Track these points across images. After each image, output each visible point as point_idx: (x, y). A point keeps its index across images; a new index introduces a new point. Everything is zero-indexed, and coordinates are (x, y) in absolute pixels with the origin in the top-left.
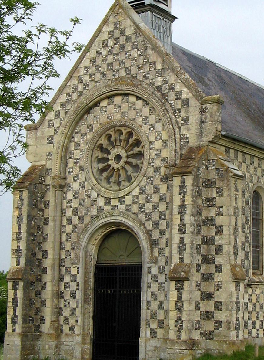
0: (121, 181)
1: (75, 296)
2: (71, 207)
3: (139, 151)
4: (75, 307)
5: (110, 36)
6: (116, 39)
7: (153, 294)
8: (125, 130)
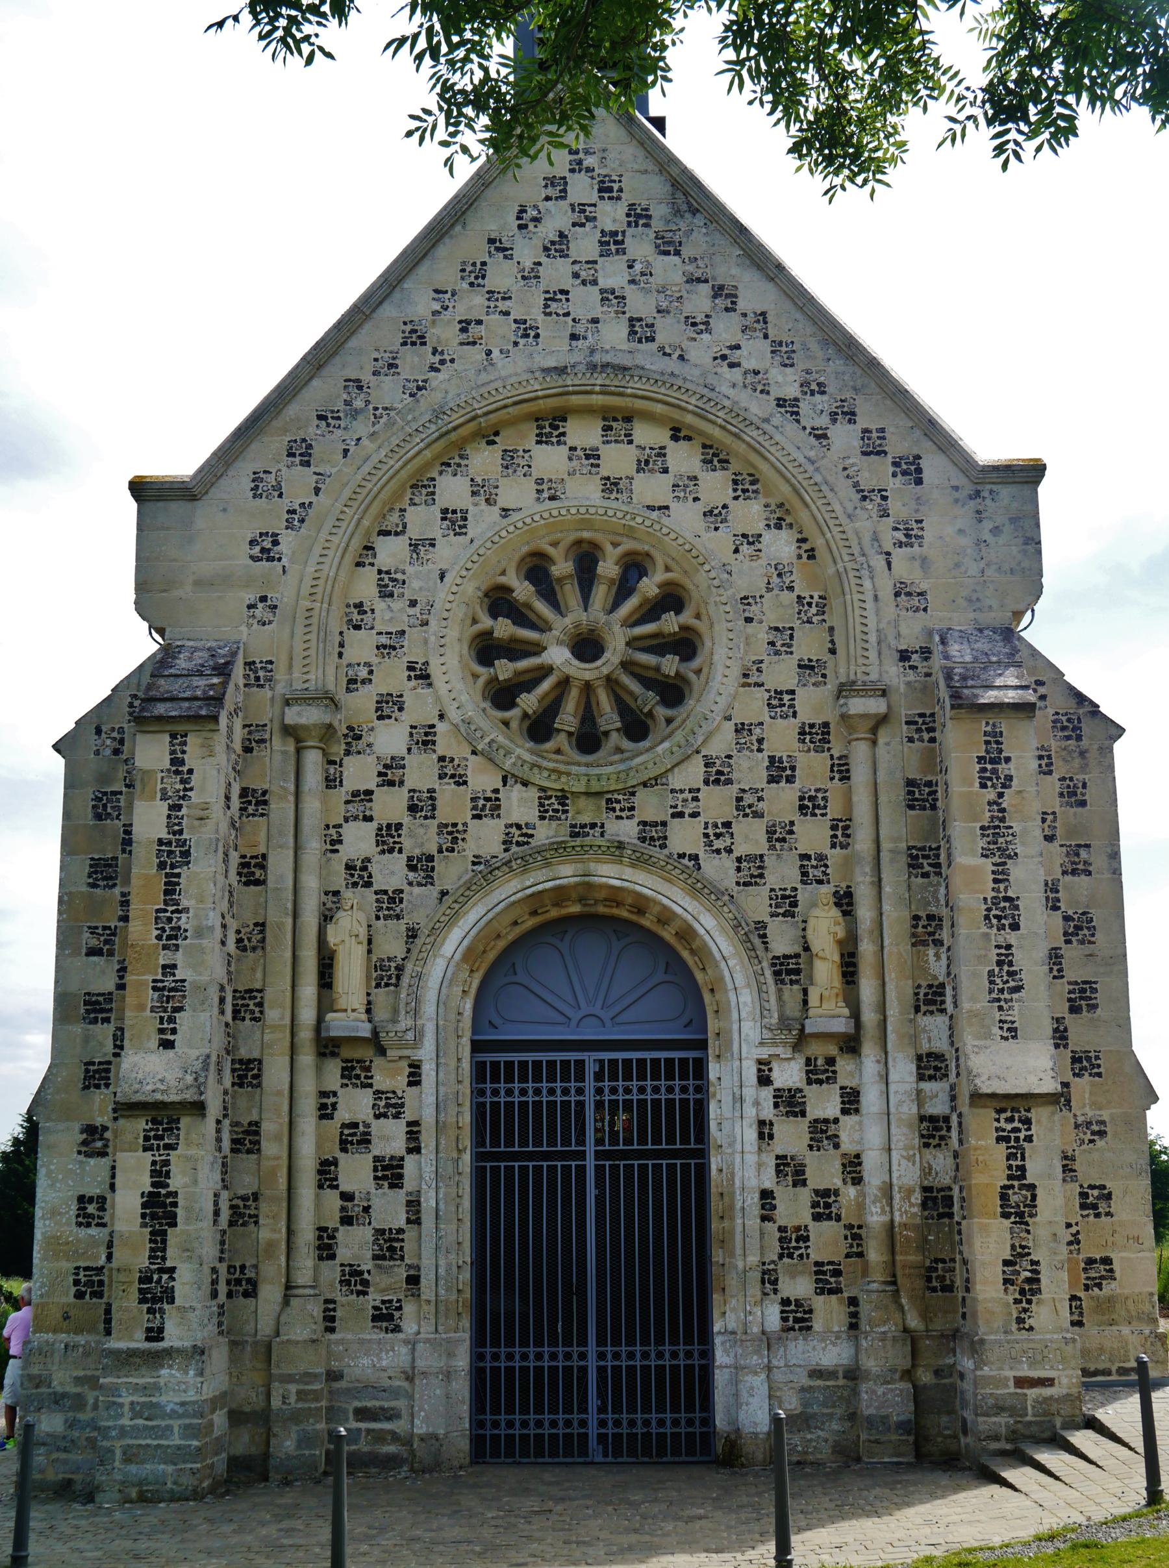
0: (606, 734)
1: (401, 1176)
2: (368, 819)
3: (684, 628)
4: (401, 1222)
5: (550, 191)
6: (581, 208)
7: (782, 1162)
8: (615, 545)
